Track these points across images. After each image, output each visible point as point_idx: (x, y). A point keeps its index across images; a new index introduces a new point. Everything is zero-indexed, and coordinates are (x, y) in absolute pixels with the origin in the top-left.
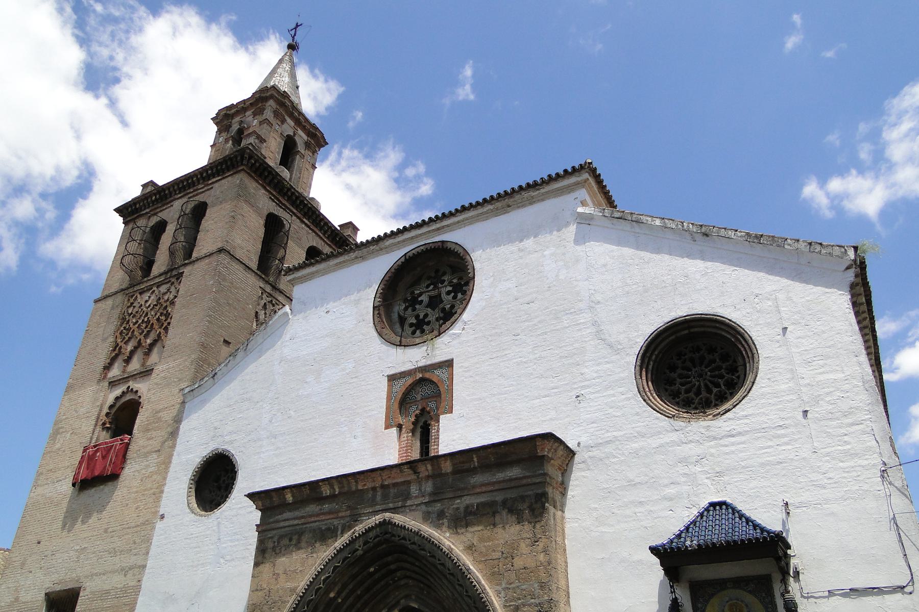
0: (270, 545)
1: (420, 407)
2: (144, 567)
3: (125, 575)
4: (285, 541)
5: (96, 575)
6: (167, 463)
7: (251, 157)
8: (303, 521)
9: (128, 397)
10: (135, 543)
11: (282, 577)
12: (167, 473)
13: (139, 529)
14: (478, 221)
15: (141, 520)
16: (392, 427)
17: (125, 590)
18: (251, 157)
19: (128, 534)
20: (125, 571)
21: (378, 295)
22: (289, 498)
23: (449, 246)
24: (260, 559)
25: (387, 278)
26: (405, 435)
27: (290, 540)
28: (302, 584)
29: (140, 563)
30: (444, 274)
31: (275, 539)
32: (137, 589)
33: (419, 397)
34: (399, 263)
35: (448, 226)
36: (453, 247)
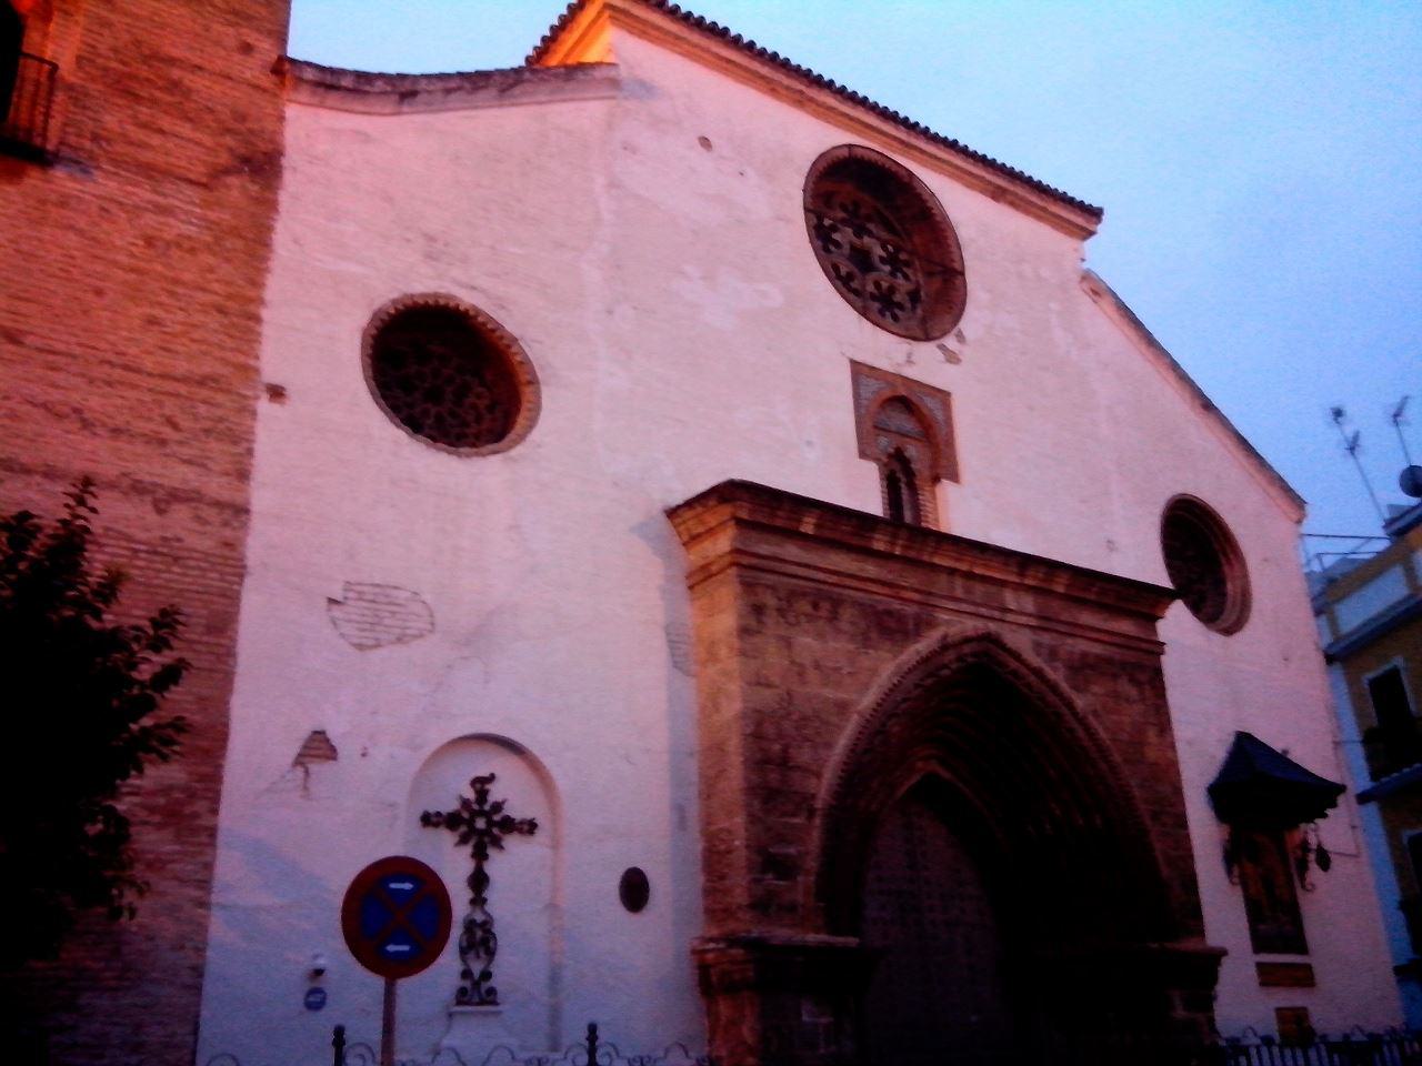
0: (771, 601)
4: (805, 606)
8: (834, 579)
10: (175, 426)
11: (812, 675)
13: (183, 389)
15: (182, 367)
19: (134, 387)
22: (808, 526)
24: (752, 623)
27: (815, 606)
28: (868, 700)
29: (216, 487)
35: (922, 152)
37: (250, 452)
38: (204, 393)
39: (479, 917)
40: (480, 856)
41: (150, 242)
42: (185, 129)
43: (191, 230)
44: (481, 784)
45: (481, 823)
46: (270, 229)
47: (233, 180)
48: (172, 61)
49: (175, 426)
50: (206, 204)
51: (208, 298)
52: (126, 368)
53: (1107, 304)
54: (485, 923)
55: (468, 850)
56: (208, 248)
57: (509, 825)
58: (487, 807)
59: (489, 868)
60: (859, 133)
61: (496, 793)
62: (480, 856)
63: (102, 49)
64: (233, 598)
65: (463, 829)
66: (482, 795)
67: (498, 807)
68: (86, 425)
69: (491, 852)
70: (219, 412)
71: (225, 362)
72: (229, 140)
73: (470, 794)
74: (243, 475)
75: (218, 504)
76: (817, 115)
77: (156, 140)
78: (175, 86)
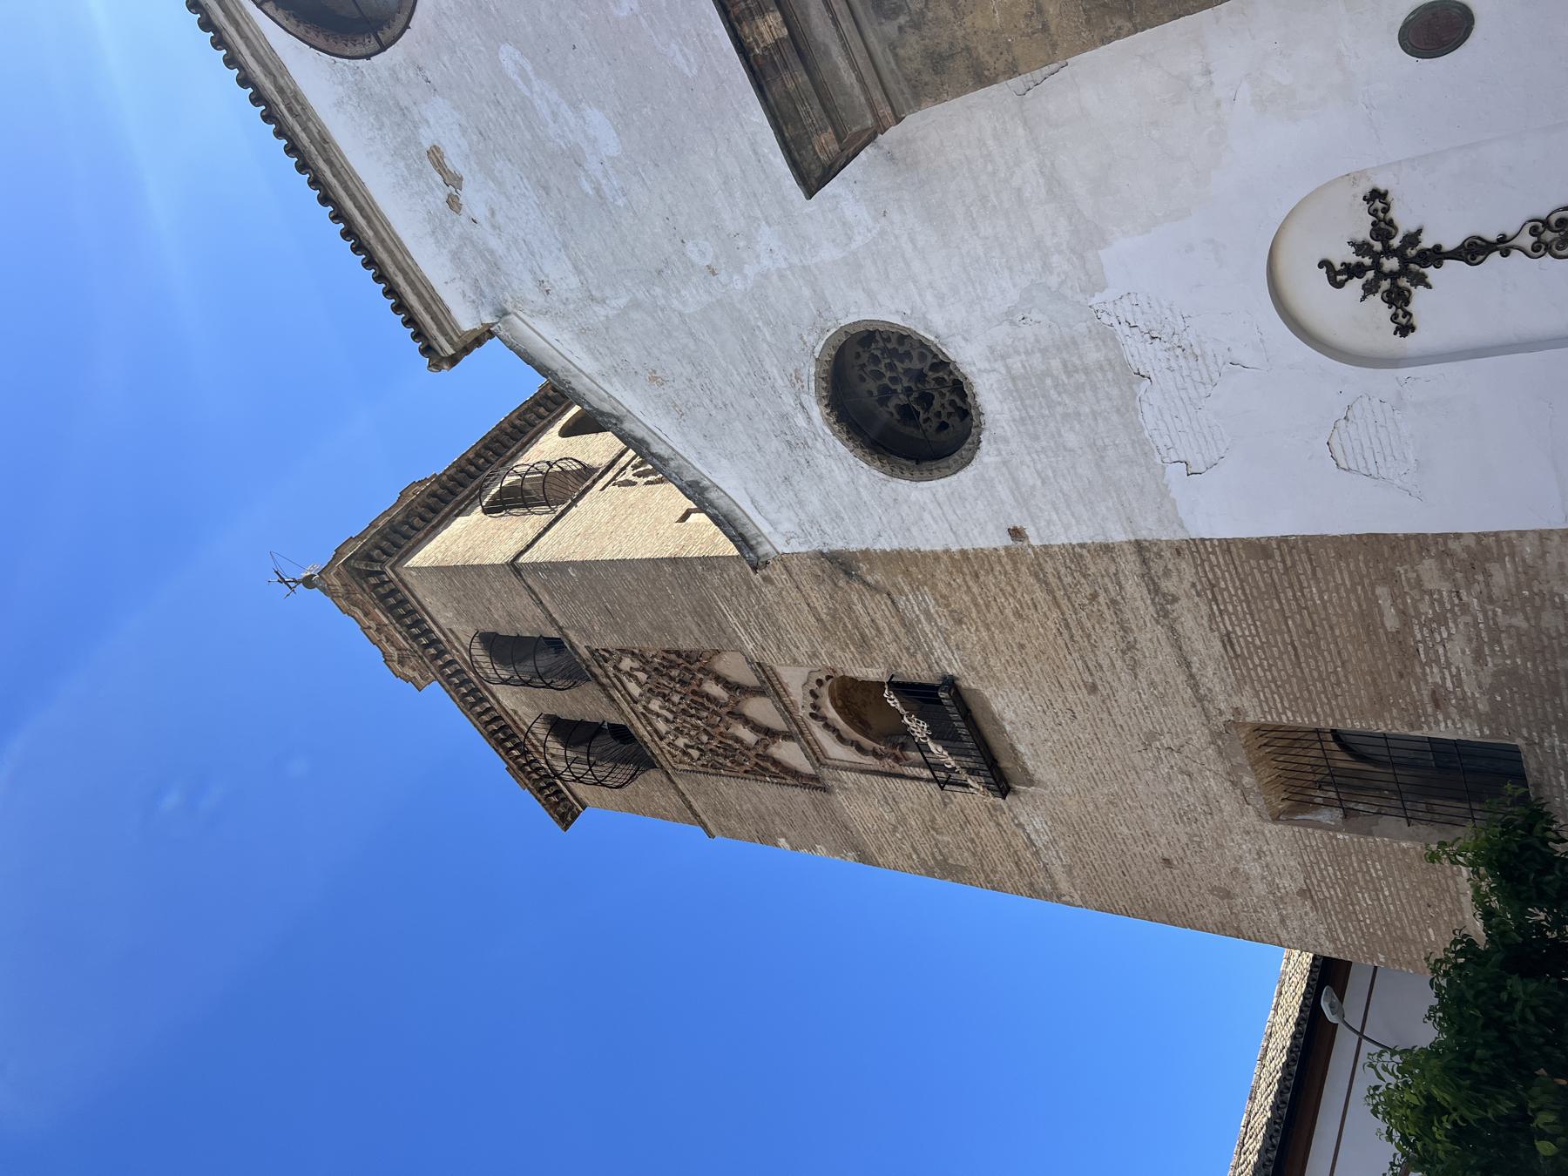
0: (913, 46)
2: (1140, 547)
3: (1175, 599)
5: (1195, 687)
6: (904, 561)
7: (369, 558)
9: (832, 714)
12: (925, 555)
13: (1060, 594)
15: (1040, 595)
17: (1210, 590)
18: (369, 558)
19: (1079, 622)
20: (1164, 604)
22: (770, 27)
25: (321, 41)
29: (1130, 565)
31: (890, 28)
32: (1196, 549)
37: (1082, 546)
38: (1052, 580)
39: (1527, 240)
40: (1436, 256)
41: (960, 622)
42: (859, 608)
43: (931, 604)
44: (1337, 275)
45: (1391, 264)
46: (884, 552)
47: (869, 578)
48: (819, 620)
49: (1094, 596)
50: (901, 592)
51: (975, 590)
52: (1067, 626)
54: (1534, 231)
55: (1431, 272)
56: (934, 587)
57: (1383, 228)
58: (1367, 261)
59: (1449, 244)
61: (1343, 255)
62: (1436, 256)
63: (849, 656)
64: (1227, 545)
65: (1403, 282)
66: (1353, 271)
67: (1361, 248)
68: (1131, 647)
69: (1427, 242)
70: (1063, 571)
71: (1016, 569)
72: (841, 583)
73: (1356, 285)
74: (1106, 549)
75: (1144, 562)
76: (282, 67)
77: (882, 624)
78: (834, 615)
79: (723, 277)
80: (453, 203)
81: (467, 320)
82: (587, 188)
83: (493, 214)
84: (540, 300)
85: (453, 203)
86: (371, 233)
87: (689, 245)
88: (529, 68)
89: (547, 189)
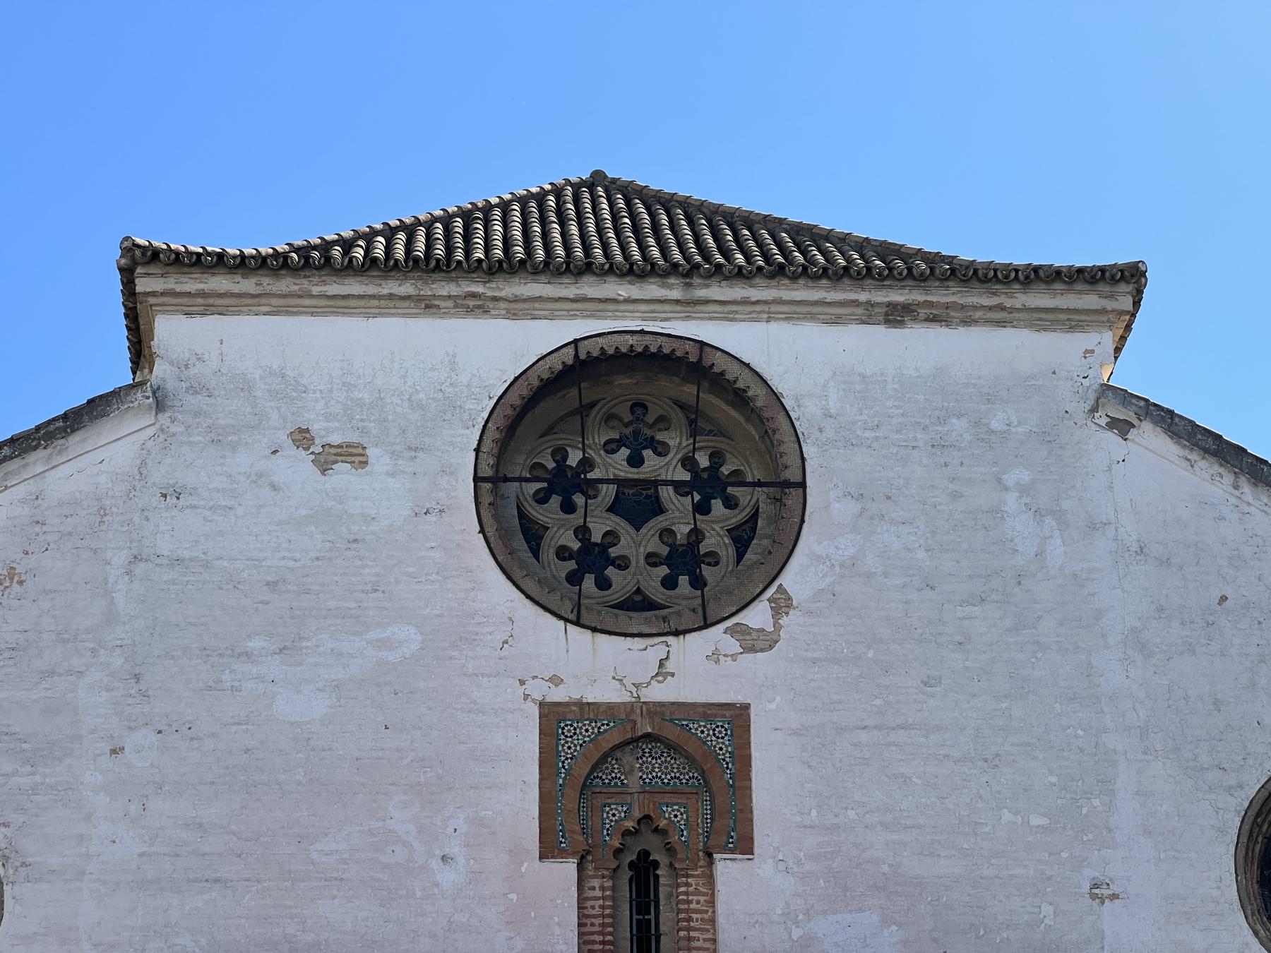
1: (637, 814)
14: (811, 317)
16: (563, 854)
21: (488, 443)
23: (720, 363)
26: (596, 883)
30: (663, 422)
33: (634, 783)
34: (556, 363)
36: (733, 371)
53: (1148, 436)
60: (593, 315)
76: (513, 315)
79: (106, 762)
80: (302, 437)
81: (170, 331)
82: (255, 644)
83: (274, 487)
84: (159, 475)
85: (302, 437)
86: (316, 290)
87: (153, 738)
88: (391, 657)
89: (272, 585)
